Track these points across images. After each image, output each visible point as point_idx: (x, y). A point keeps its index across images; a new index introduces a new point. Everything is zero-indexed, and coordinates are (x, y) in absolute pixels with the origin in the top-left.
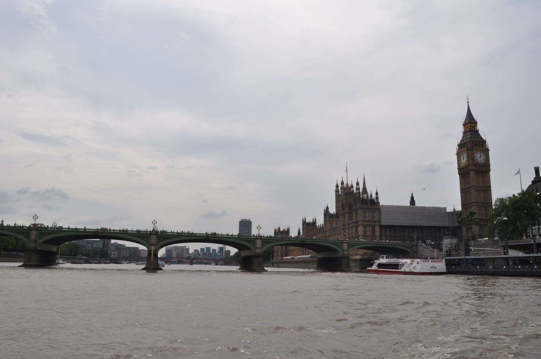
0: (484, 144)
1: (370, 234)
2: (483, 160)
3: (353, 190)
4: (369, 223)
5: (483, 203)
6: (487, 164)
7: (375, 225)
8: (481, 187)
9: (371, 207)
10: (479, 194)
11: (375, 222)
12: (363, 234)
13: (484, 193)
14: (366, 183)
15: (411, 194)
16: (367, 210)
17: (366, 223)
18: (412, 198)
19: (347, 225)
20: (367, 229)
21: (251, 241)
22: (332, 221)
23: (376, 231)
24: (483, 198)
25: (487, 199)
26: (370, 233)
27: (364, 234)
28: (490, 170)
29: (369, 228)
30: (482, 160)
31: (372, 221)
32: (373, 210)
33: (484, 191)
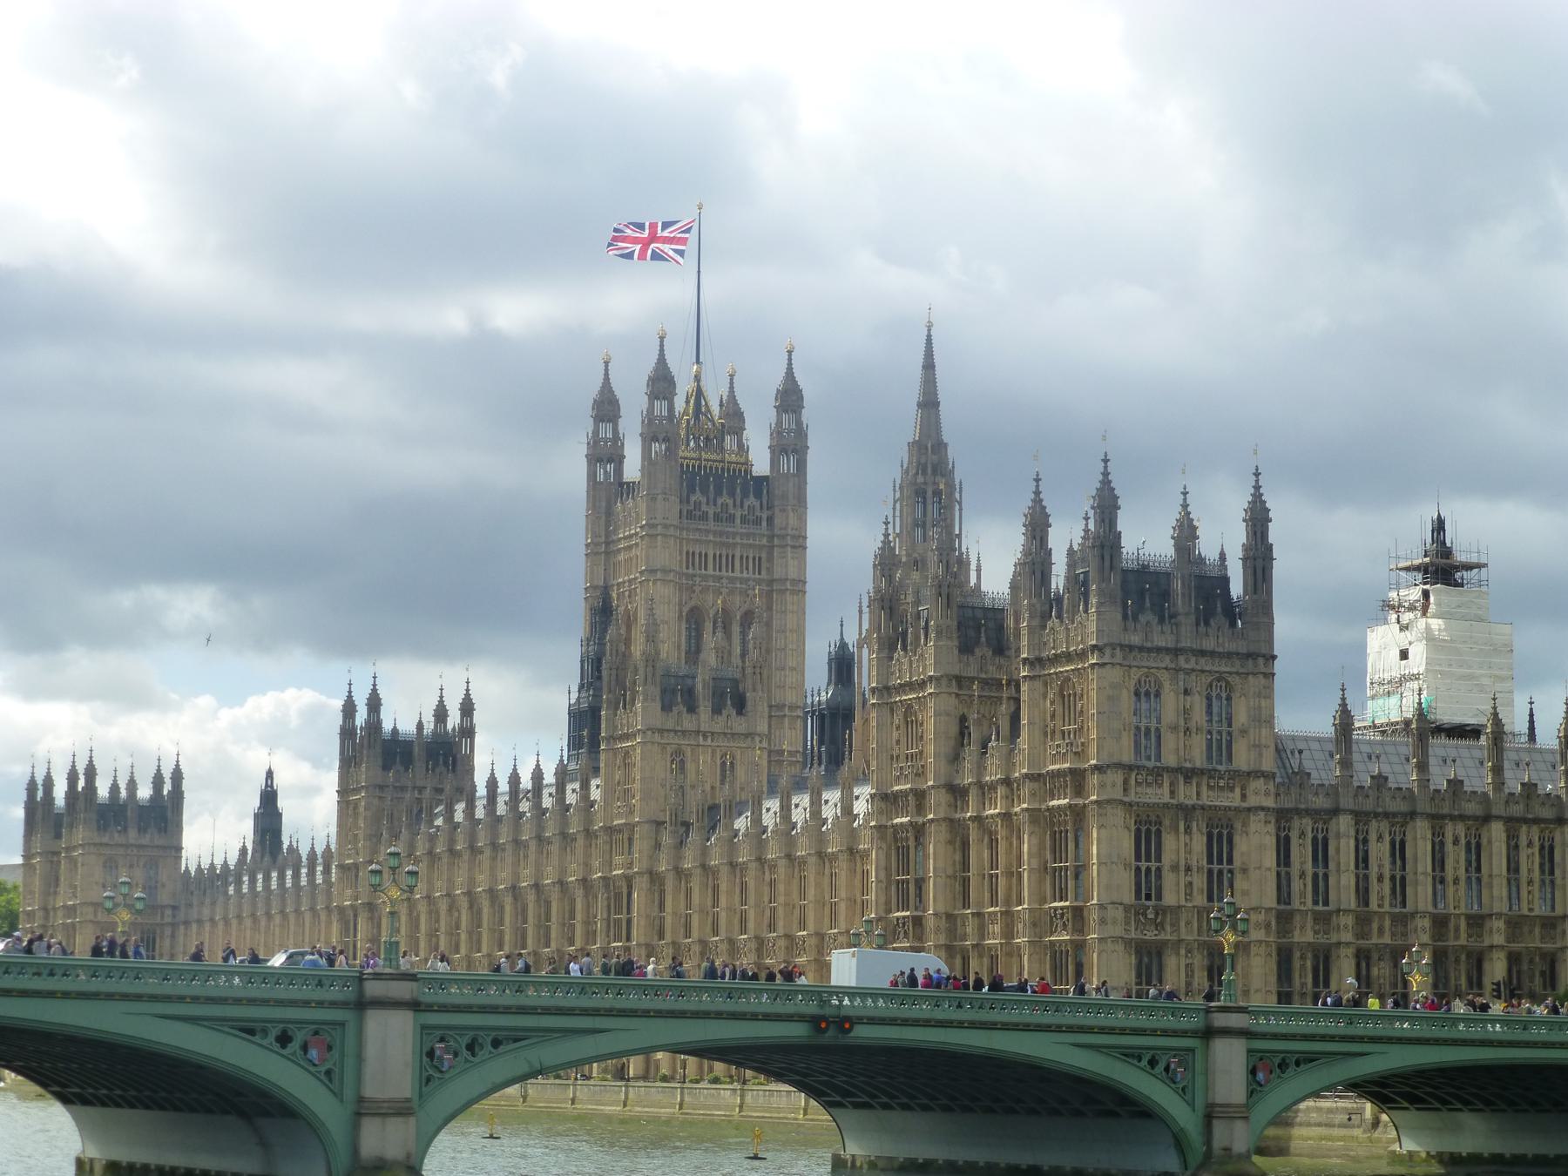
1: (1189, 895)
3: (742, 449)
9: (1209, 644)
11: (1232, 789)
12: (1128, 897)
14: (941, 397)
17: (1159, 795)
21: (302, 1023)
23: (1245, 871)
29: (1182, 837)
31: (1210, 773)
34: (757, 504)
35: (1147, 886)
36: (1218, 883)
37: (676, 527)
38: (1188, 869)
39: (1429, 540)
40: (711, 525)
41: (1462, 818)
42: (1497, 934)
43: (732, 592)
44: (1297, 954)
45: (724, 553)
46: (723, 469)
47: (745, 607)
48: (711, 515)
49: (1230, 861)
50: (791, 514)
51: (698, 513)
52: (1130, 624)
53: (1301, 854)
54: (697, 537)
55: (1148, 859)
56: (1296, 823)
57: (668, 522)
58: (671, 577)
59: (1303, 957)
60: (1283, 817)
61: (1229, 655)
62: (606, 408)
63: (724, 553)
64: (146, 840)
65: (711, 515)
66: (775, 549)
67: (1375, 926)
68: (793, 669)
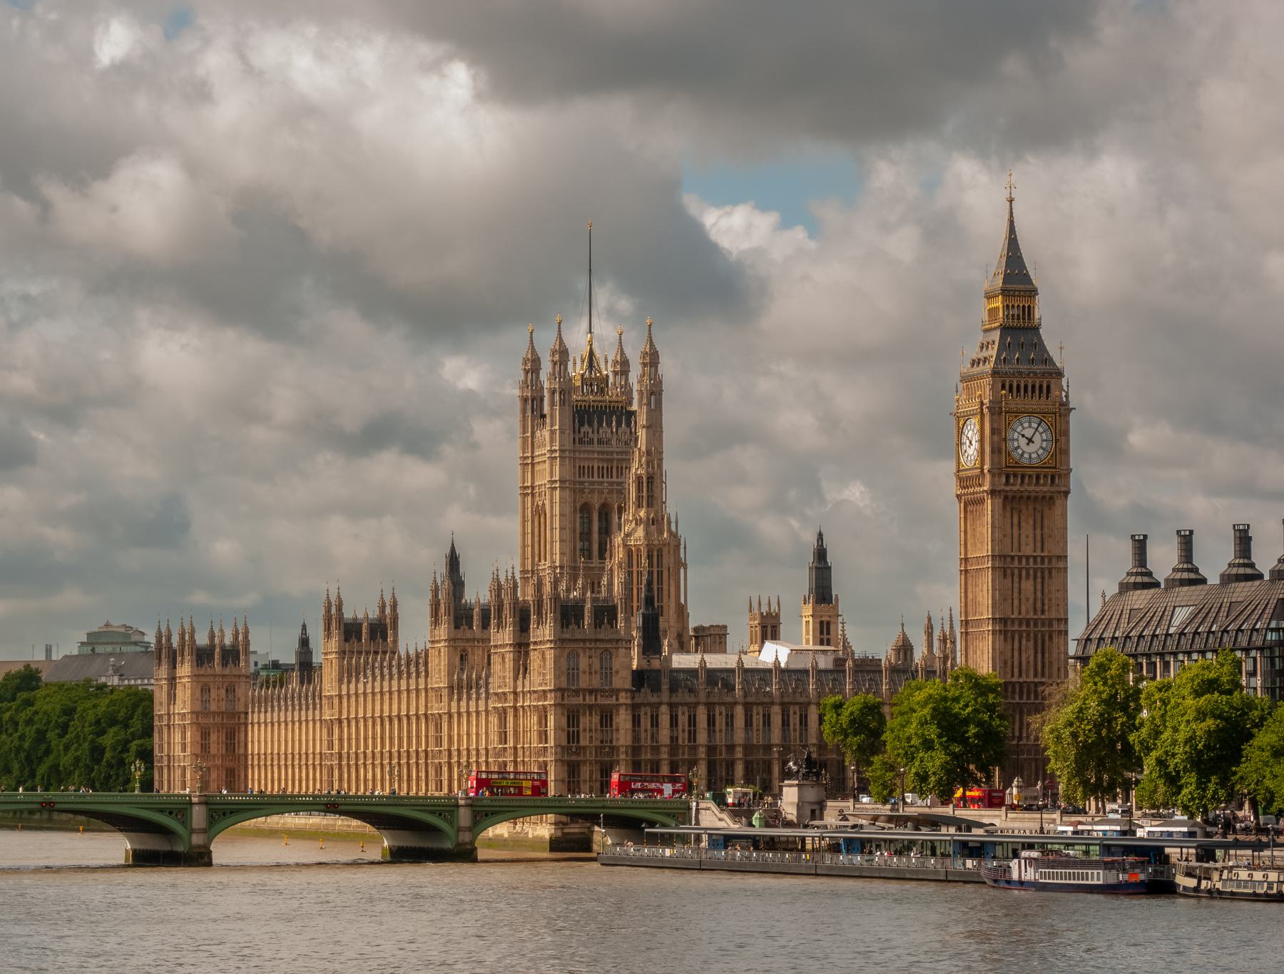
1: (591, 741)
2: (1041, 452)
6: (1055, 468)
7: (613, 705)
8: (1028, 558)
9: (601, 636)
10: (1016, 585)
11: (612, 696)
13: (1039, 580)
16: (584, 649)
18: (821, 554)
20: (582, 720)
22: (468, 640)
23: (617, 730)
24: (1031, 601)
25: (1046, 607)
27: (569, 742)
28: (1067, 493)
31: (602, 691)
32: (608, 646)
33: (1039, 574)
38: (591, 730)
39: (816, 545)
40: (596, 447)
42: (739, 754)
43: (611, 492)
44: (643, 764)
45: (605, 466)
49: (611, 726)
51: (586, 439)
52: (565, 629)
53: (645, 722)
54: (586, 456)
55: (573, 727)
57: (567, 447)
58: (567, 485)
59: (646, 765)
60: (635, 708)
61: (610, 641)
63: (605, 466)
64: (227, 672)
67: (681, 751)
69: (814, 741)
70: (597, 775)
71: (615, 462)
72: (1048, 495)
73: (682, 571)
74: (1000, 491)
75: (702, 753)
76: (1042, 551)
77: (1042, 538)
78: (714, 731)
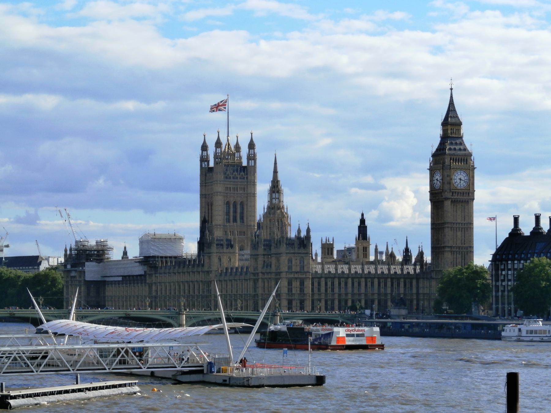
0: (468, 160)
3: (240, 158)
4: (295, 274)
5: (461, 248)
7: (305, 278)
8: (459, 223)
9: (300, 252)
10: (455, 234)
11: (304, 274)
12: (287, 292)
13: (463, 232)
15: (361, 215)
17: (292, 276)
18: (363, 221)
19: (260, 275)
22: (221, 253)
23: (306, 287)
25: (465, 242)
26: (297, 290)
28: (473, 199)
30: (463, 184)
31: (301, 272)
32: (303, 255)
33: (463, 230)
34: (244, 174)
35: (290, 290)
36: (302, 290)
37: (223, 181)
40: (232, 180)
41: (344, 278)
45: (235, 187)
46: (235, 165)
47: (241, 201)
48: (232, 176)
49: (304, 286)
50: (252, 176)
51: (228, 177)
53: (316, 284)
56: (315, 279)
62: (204, 147)
63: (235, 187)
65: (232, 176)
66: (249, 185)
68: (253, 216)
69: (376, 292)
70: (298, 304)
71: (239, 185)
72: (467, 200)
73: (289, 227)
74: (449, 199)
75: (336, 296)
76: (464, 221)
77: (464, 217)
78: (354, 288)
